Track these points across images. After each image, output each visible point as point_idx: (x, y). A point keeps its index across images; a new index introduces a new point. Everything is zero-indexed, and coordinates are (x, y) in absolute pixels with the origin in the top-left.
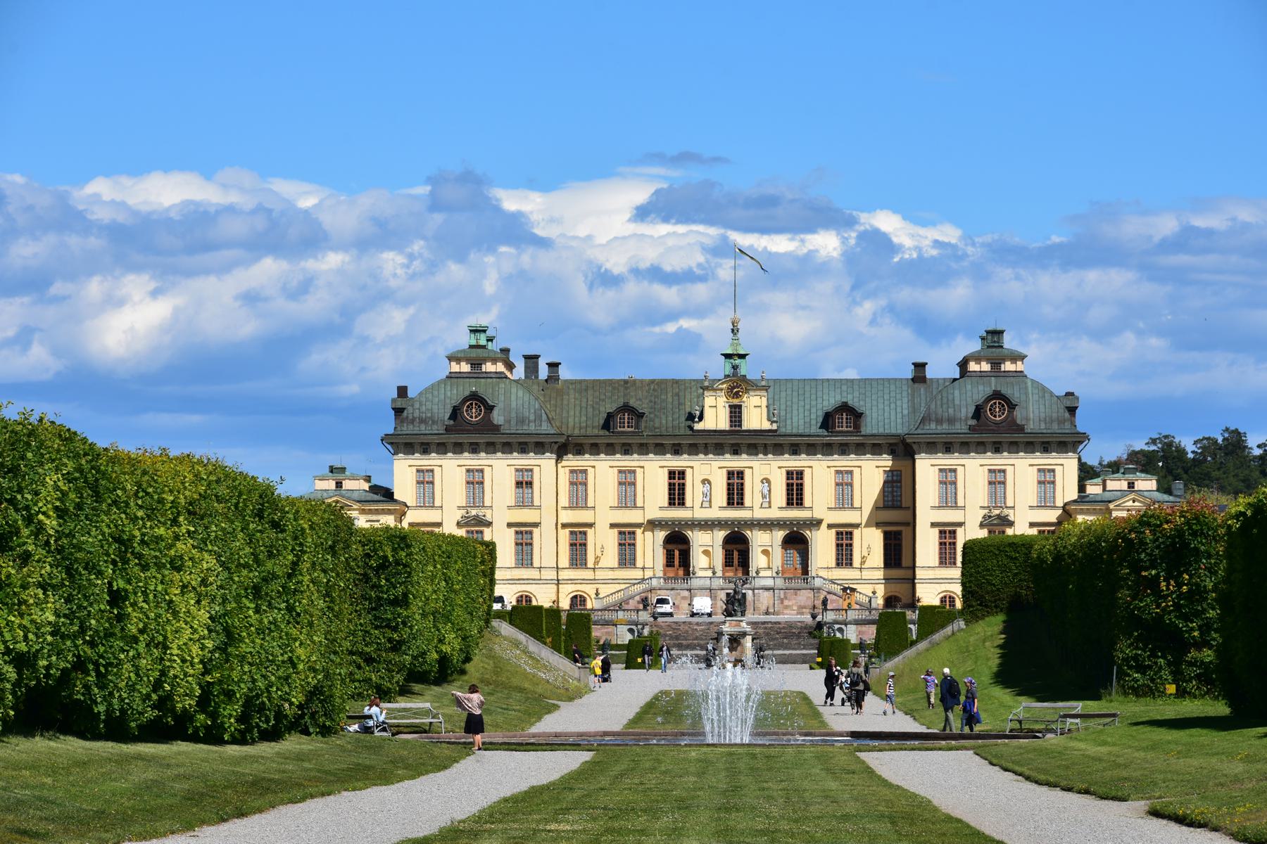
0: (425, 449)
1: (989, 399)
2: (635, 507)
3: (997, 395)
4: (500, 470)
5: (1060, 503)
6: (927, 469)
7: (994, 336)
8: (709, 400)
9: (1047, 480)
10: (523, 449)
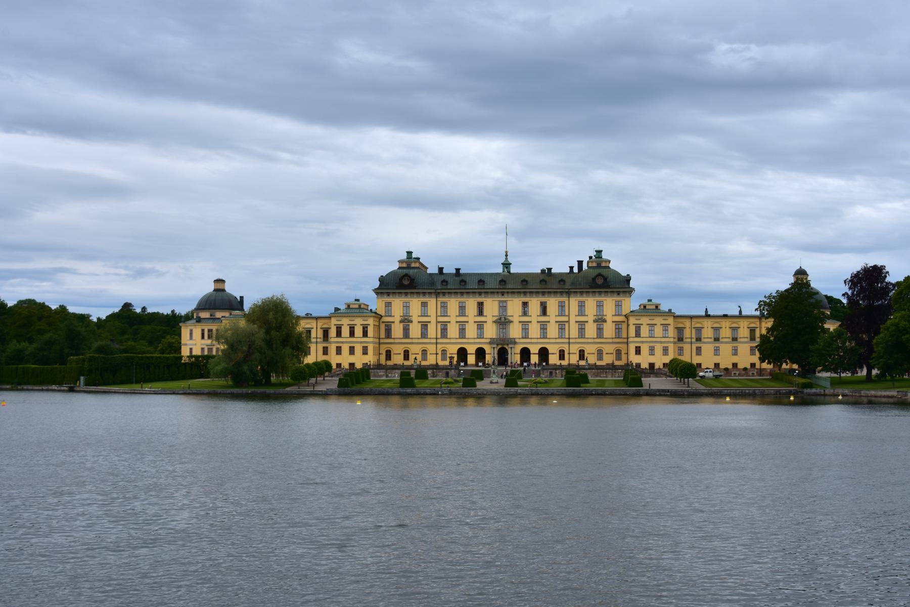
0: (388, 294)
1: (597, 276)
3: (600, 275)
4: (415, 303)
5: (624, 313)
6: (573, 303)
7: (599, 252)
9: (618, 305)
10: (424, 294)
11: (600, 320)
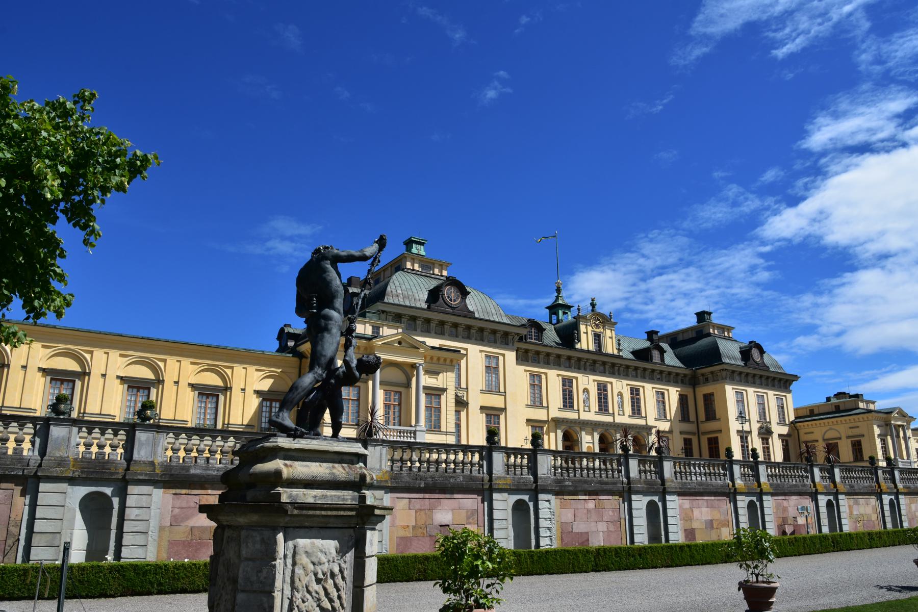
2: (541, 406)
8: (583, 328)
11: (765, 433)
